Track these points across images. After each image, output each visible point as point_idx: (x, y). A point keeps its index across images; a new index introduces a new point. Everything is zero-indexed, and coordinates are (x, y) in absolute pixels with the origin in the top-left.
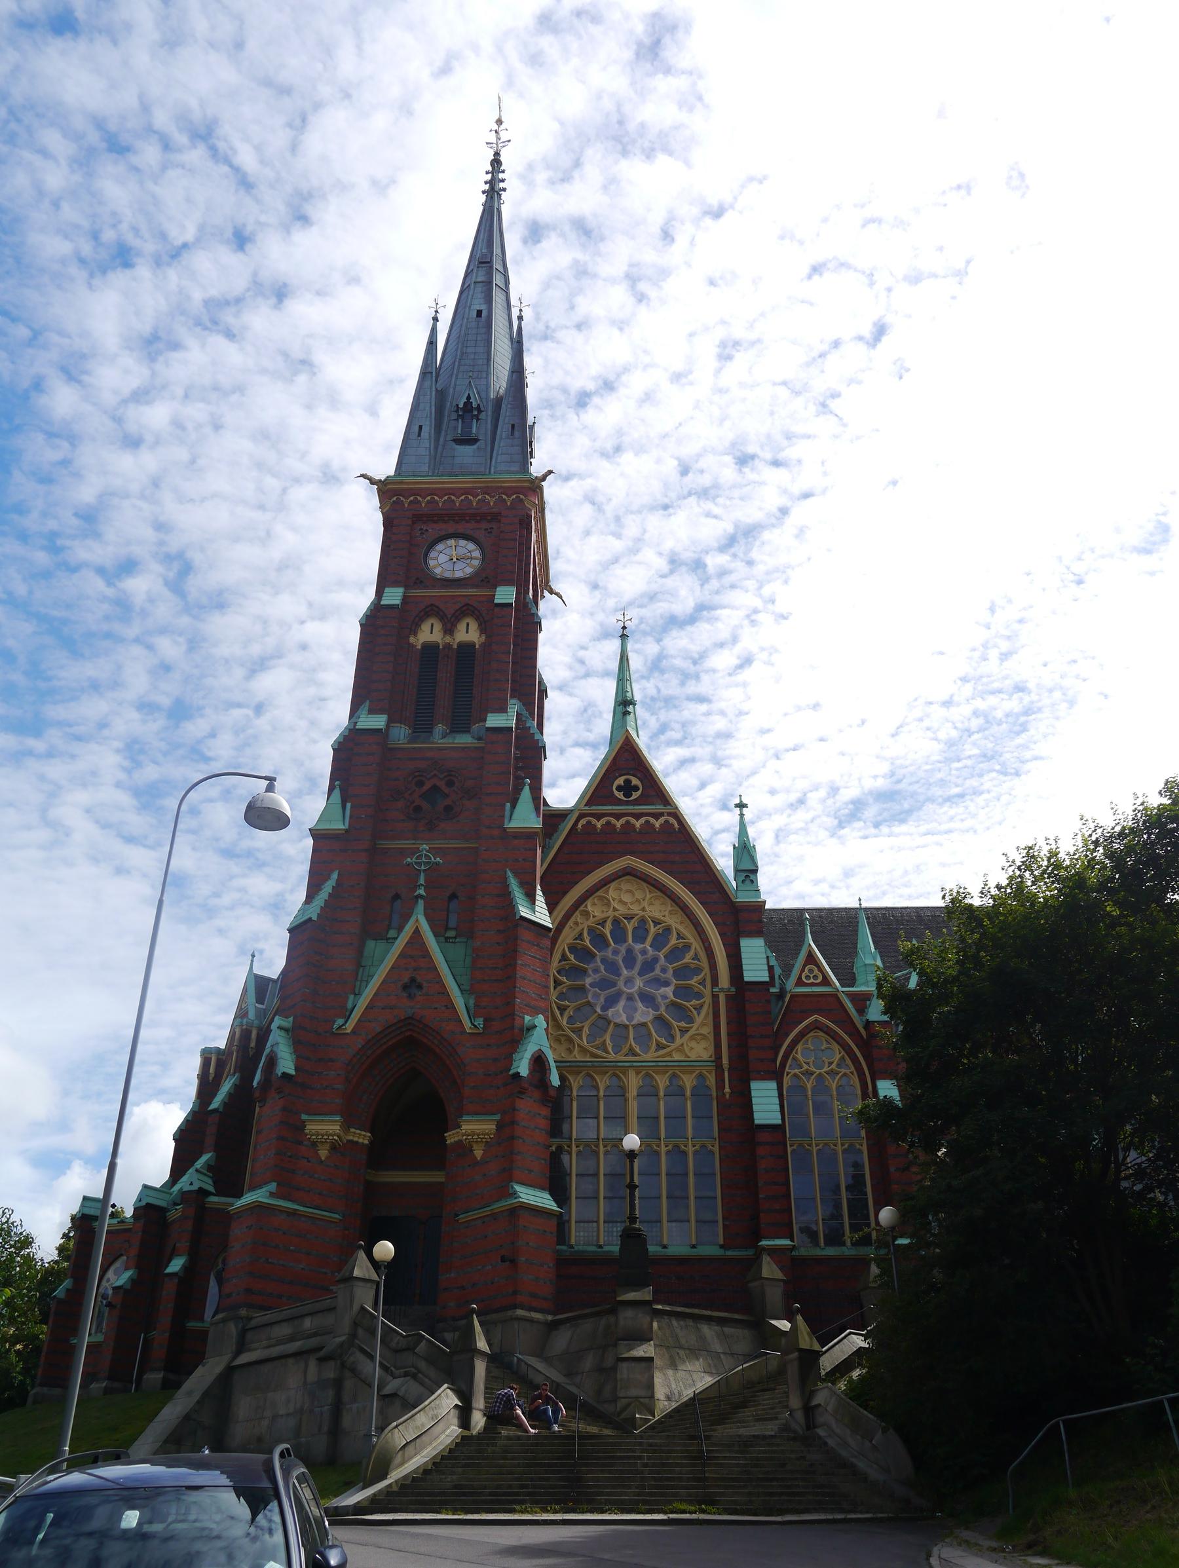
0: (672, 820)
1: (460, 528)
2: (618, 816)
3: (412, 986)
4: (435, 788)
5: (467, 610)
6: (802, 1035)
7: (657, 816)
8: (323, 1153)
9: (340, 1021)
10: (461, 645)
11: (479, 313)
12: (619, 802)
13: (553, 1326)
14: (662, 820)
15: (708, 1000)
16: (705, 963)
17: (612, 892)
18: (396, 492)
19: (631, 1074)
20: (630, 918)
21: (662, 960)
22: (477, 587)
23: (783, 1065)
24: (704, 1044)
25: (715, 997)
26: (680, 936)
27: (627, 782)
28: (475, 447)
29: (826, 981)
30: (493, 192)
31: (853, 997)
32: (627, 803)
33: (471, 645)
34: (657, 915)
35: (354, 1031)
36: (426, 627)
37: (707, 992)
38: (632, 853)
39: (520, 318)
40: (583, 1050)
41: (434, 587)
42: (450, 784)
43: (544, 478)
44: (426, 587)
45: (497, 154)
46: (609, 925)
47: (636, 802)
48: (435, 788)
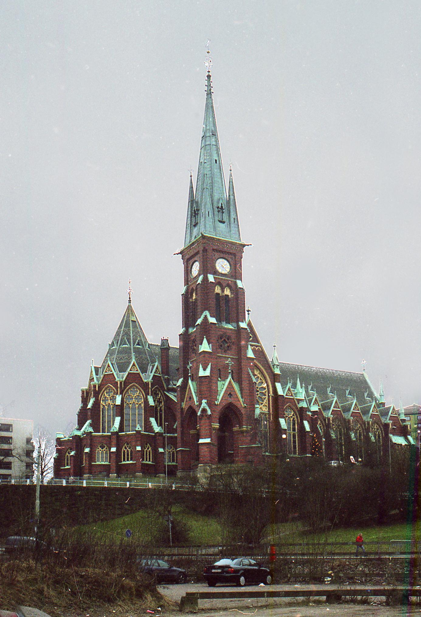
3: (230, 394)
10: (226, 295)
11: (216, 160)
33: (228, 296)
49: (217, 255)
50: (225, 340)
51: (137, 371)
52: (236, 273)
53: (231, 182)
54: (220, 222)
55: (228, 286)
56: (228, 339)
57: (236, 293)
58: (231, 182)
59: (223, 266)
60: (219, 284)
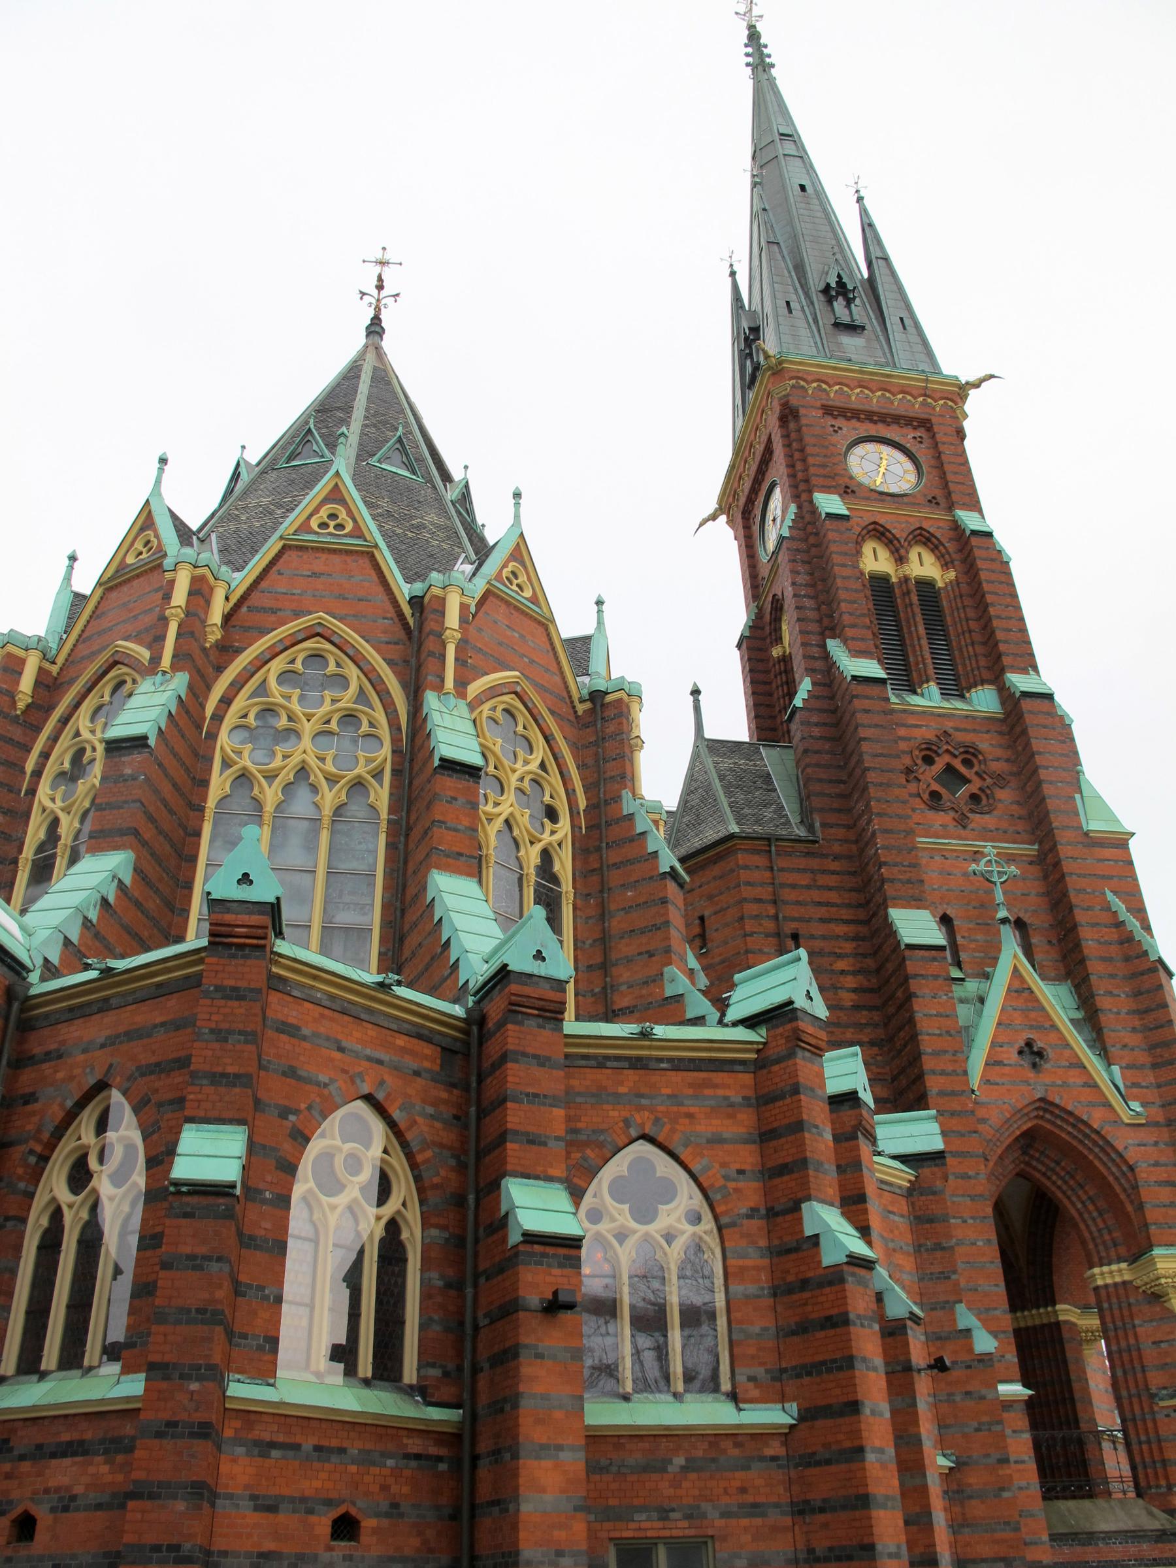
11: (803, 188)
30: (760, 65)
43: (977, 385)
45: (752, 28)
49: (850, 429)
50: (949, 768)
52: (949, 480)
53: (868, 227)
55: (924, 538)
56: (967, 763)
57: (964, 561)
58: (868, 227)
59: (882, 468)
60: (880, 533)
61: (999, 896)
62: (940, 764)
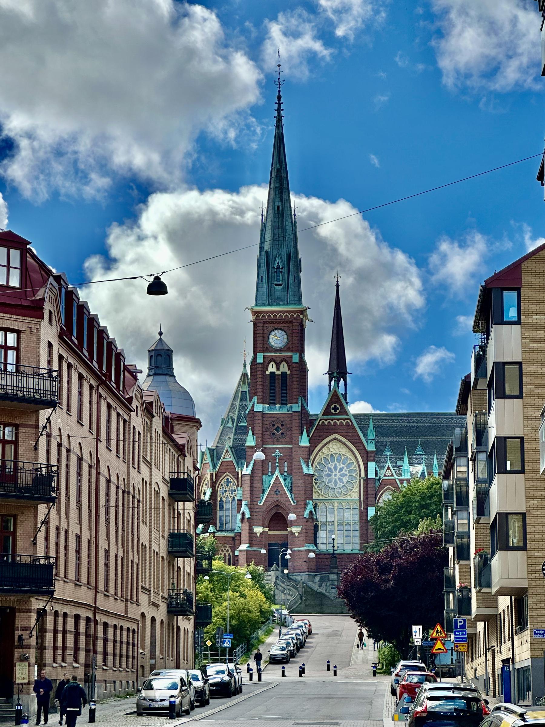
0: (349, 421)
1: (279, 326)
2: (332, 420)
3: (277, 492)
4: (278, 427)
5: (283, 360)
6: (384, 491)
7: (344, 420)
8: (258, 535)
9: (259, 501)
12: (332, 414)
13: (316, 575)
14: (346, 421)
15: (358, 480)
16: (358, 469)
17: (330, 445)
18: (256, 312)
19: (336, 503)
20: (336, 454)
21: (345, 468)
22: (285, 351)
23: (378, 500)
24: (356, 493)
25: (360, 480)
26: (351, 460)
27: (335, 406)
28: (282, 287)
29: (392, 475)
31: (400, 480)
32: (335, 415)
34: (344, 453)
35: (263, 504)
36: (270, 365)
37: (358, 478)
38: (337, 433)
39: (295, 215)
40: (322, 496)
41: (272, 351)
42: (282, 425)
44: (270, 352)
46: (329, 456)
47: (338, 414)
48: (278, 427)
51: (230, 458)
54: (277, 285)
61: (277, 461)
62: (276, 427)
